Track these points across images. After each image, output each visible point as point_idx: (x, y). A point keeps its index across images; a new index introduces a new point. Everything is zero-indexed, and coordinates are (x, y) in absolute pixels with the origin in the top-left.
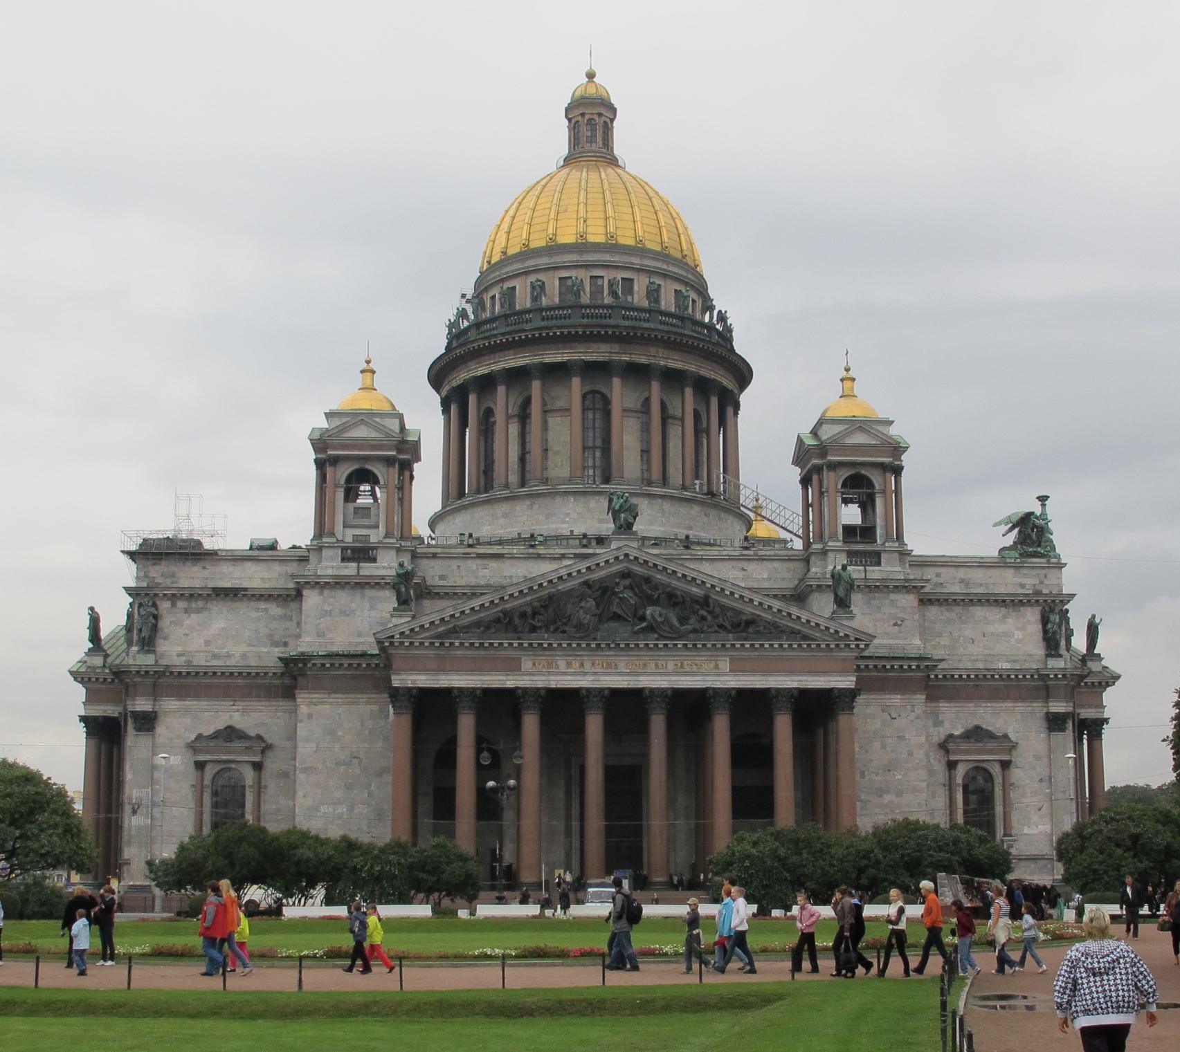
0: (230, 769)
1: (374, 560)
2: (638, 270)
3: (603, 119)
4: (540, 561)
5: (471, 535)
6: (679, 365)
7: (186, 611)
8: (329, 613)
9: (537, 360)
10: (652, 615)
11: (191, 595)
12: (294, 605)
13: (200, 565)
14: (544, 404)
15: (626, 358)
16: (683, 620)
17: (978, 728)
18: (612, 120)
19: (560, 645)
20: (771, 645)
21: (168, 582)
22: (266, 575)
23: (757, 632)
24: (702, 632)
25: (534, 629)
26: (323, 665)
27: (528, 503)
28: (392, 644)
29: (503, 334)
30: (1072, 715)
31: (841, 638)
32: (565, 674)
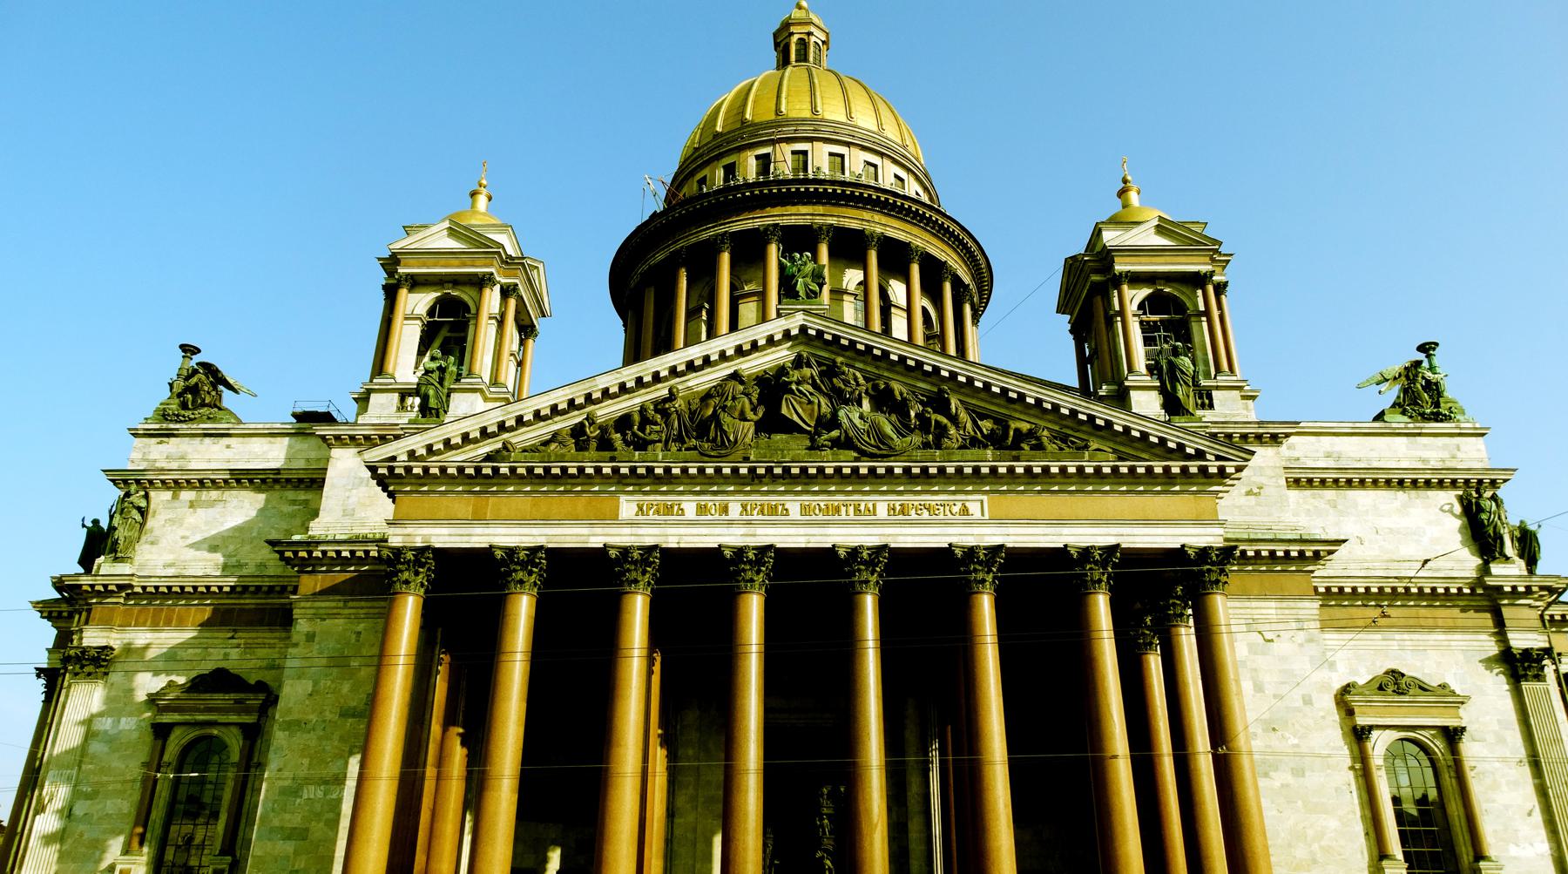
0: (211, 737)
2: (848, 144)
3: (813, 39)
6: (902, 236)
7: (192, 505)
9: (721, 230)
11: (201, 481)
13: (226, 441)
14: (733, 288)
16: (904, 428)
17: (1395, 675)
21: (174, 465)
23: (1039, 447)
24: (939, 447)
25: (641, 445)
28: (391, 469)
30: (1548, 652)
31: (1189, 457)
32: (692, 523)
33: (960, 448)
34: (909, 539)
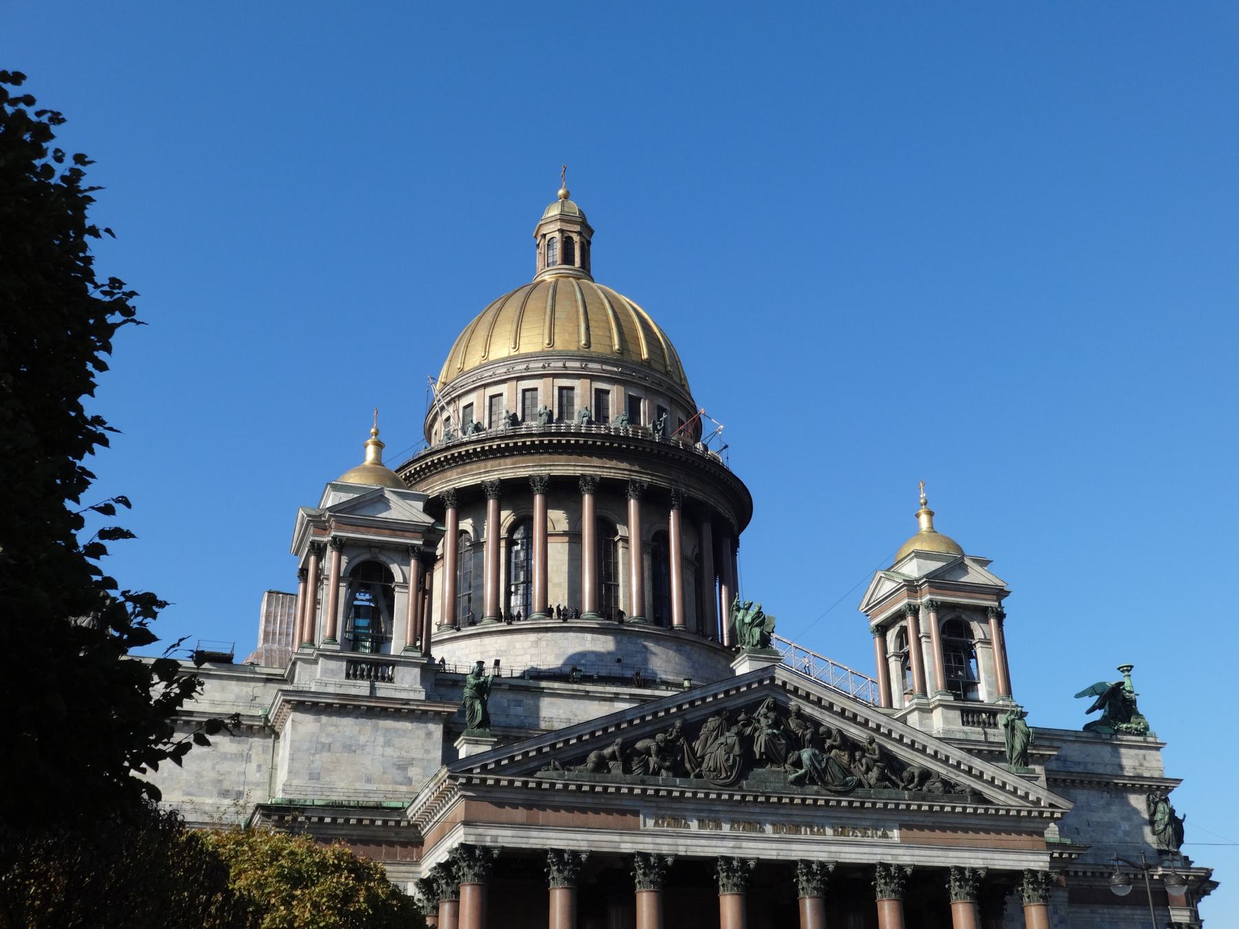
1: (391, 680)
2: (646, 389)
4: (587, 702)
5: (497, 663)
6: (700, 496)
8: (329, 747)
10: (811, 759)
12: (257, 742)
15: (646, 479)
18: (589, 243)
19: (695, 794)
20: (953, 808)
22: (218, 696)
26: (321, 819)
27: (532, 637)
28: (469, 780)
29: (502, 438)
33: (886, 787)
34: (848, 856)
